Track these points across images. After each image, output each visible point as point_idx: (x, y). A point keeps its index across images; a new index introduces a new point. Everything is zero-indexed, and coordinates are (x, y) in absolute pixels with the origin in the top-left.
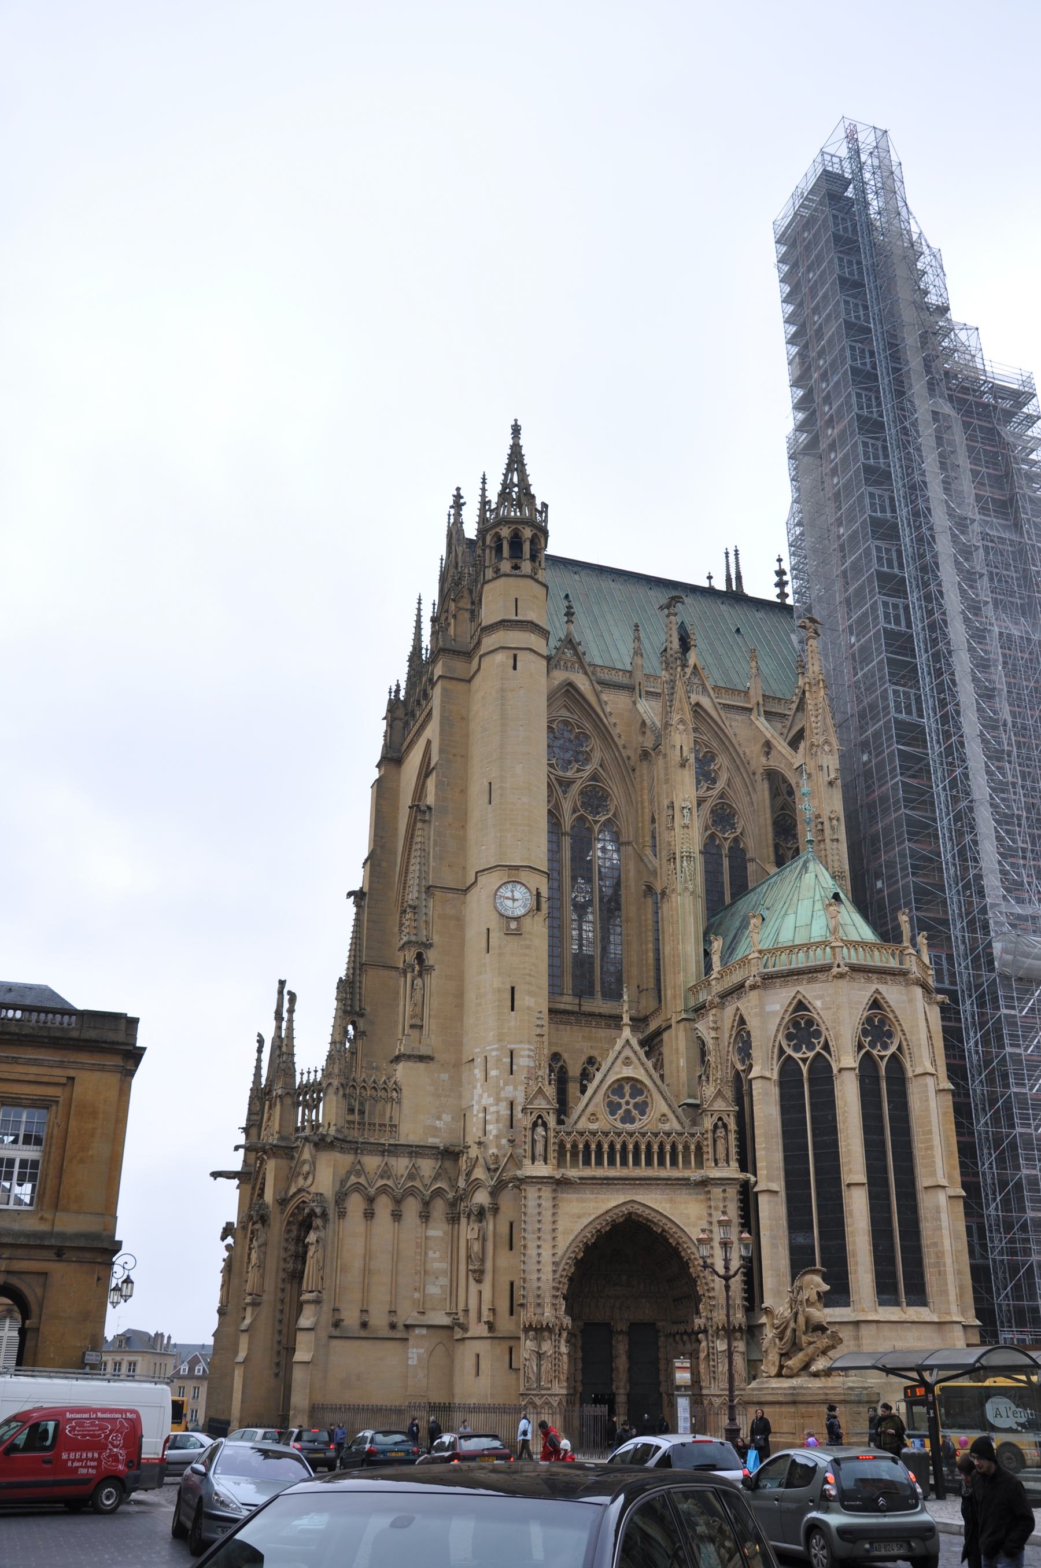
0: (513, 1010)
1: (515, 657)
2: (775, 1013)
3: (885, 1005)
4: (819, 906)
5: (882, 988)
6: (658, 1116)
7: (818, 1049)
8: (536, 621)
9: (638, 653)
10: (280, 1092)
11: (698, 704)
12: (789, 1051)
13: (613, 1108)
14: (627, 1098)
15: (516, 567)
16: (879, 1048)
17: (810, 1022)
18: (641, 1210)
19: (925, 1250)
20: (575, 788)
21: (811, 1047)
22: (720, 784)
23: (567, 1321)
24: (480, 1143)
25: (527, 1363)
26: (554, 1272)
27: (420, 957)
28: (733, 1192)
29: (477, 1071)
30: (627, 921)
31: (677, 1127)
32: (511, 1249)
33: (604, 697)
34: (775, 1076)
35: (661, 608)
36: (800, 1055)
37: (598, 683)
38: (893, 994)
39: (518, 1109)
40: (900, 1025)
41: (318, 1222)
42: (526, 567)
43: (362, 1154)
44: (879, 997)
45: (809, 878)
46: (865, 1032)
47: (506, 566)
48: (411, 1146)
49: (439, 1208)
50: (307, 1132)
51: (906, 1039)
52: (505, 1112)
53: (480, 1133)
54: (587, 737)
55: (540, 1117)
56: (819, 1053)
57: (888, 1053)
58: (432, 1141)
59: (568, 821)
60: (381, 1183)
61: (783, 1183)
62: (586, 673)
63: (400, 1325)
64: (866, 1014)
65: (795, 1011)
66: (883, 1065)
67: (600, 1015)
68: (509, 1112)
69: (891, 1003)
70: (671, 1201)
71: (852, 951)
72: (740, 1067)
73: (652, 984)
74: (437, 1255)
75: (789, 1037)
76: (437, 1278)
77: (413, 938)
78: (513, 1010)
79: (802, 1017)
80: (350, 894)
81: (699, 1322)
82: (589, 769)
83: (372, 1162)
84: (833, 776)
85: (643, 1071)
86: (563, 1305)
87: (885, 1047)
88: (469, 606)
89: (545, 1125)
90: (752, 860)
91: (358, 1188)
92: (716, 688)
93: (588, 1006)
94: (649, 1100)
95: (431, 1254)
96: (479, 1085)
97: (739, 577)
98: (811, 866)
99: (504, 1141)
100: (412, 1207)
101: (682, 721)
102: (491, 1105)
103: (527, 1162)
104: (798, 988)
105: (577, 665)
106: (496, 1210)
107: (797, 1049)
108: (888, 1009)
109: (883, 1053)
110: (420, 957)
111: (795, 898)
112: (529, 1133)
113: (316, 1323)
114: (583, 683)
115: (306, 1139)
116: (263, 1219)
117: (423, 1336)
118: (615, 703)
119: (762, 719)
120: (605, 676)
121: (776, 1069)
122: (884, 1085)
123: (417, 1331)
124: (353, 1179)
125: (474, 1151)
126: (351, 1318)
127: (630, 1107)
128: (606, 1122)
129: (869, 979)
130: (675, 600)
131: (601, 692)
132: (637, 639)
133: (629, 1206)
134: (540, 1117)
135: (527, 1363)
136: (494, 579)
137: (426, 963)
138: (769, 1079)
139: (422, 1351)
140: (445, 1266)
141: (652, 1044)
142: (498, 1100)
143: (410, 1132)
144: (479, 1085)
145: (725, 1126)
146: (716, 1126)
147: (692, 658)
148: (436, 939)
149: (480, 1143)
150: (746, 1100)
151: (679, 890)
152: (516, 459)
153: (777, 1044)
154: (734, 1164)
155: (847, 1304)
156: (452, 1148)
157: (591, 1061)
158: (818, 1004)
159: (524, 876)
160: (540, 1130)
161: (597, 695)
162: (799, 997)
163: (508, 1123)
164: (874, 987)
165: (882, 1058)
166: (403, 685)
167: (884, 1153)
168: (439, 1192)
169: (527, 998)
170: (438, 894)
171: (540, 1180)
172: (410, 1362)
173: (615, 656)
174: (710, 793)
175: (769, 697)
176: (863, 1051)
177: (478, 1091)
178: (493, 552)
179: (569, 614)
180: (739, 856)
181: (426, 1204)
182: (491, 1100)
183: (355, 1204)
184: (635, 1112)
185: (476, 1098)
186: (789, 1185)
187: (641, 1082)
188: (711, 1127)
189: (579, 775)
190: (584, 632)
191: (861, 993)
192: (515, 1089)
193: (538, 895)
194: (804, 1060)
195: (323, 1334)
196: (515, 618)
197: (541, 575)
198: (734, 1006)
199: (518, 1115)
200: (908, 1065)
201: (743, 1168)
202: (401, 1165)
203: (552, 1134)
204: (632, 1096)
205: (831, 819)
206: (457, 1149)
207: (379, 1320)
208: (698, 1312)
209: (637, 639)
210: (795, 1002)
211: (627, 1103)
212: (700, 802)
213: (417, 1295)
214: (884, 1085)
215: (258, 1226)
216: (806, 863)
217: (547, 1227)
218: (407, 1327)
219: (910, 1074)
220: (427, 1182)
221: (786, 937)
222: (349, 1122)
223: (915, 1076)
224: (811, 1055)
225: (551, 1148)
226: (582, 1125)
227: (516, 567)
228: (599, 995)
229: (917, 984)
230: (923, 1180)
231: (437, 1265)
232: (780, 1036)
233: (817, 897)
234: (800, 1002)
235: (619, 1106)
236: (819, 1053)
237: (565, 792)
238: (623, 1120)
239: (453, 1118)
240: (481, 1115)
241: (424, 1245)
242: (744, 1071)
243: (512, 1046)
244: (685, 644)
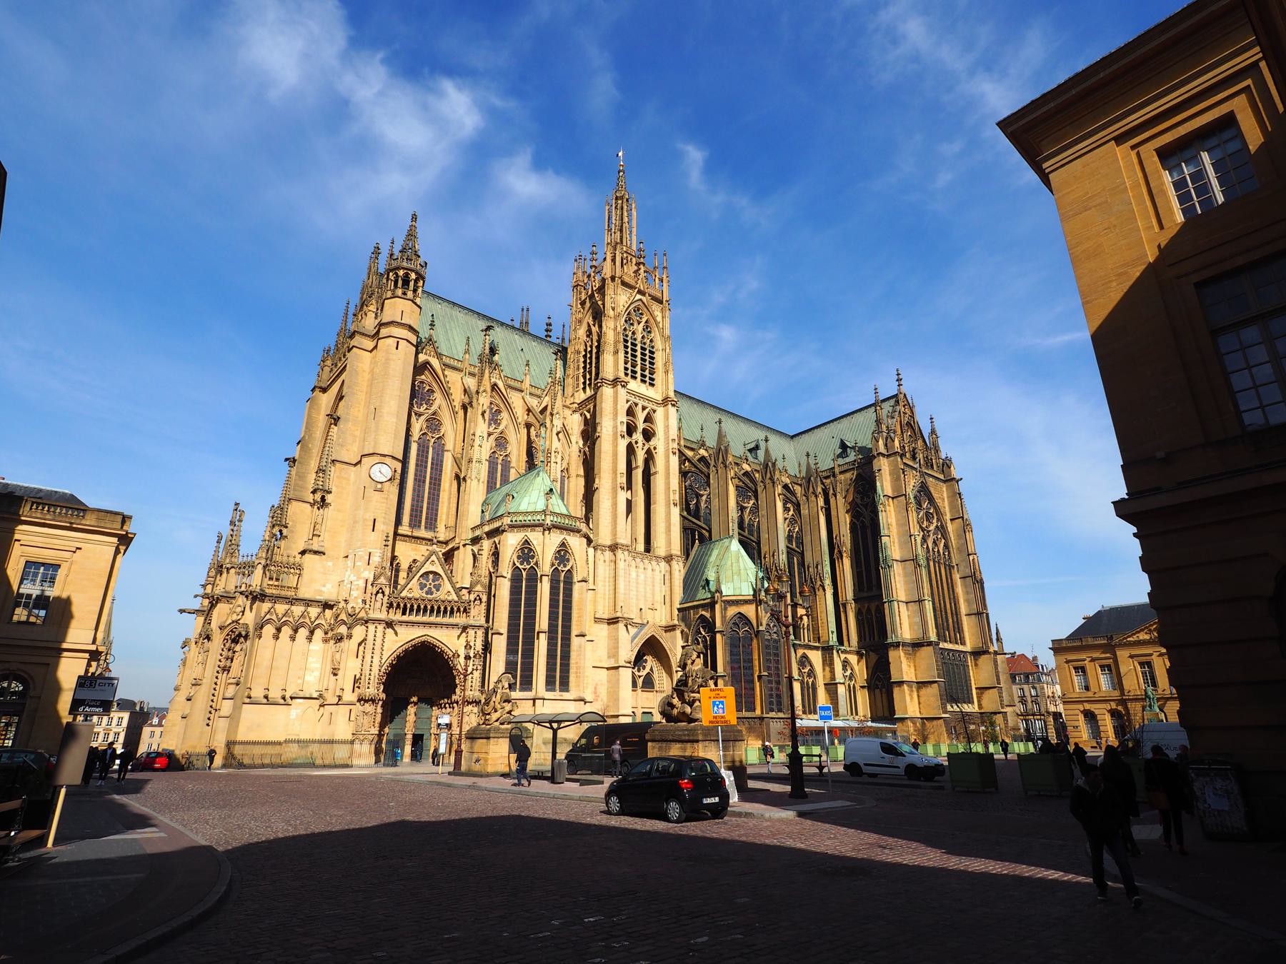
0: (373, 531)
1: (398, 342)
2: (512, 545)
4: (542, 494)
5: (567, 538)
6: (446, 592)
7: (532, 564)
8: (412, 325)
9: (467, 352)
10: (229, 566)
11: (495, 384)
12: (518, 564)
13: (422, 587)
14: (430, 581)
15: (404, 294)
17: (531, 550)
18: (430, 639)
19: (571, 665)
20: (423, 418)
21: (529, 563)
22: (501, 427)
23: (383, 696)
24: (346, 601)
25: (358, 718)
26: (380, 671)
27: (323, 498)
28: (480, 633)
29: (349, 562)
30: (443, 491)
31: (456, 599)
32: (357, 657)
33: (446, 373)
34: (509, 576)
35: (482, 331)
36: (523, 567)
37: (444, 365)
38: (576, 543)
39: (369, 583)
41: (242, 640)
42: (410, 294)
43: (275, 602)
45: (539, 480)
46: (556, 558)
47: (399, 292)
48: (305, 600)
49: (319, 634)
50: (243, 589)
52: (362, 584)
53: (347, 596)
54: (433, 391)
55: (381, 588)
56: (532, 567)
57: (566, 569)
58: (318, 598)
59: (416, 434)
60: (284, 619)
61: (506, 630)
62: (437, 358)
63: (287, 697)
64: (558, 549)
65: (522, 545)
66: (563, 574)
67: (423, 539)
68: (365, 585)
69: (571, 545)
70: (447, 636)
71: (555, 518)
72: (492, 570)
73: (453, 524)
74: (314, 660)
75: (519, 557)
76: (313, 672)
77: (321, 487)
78: (373, 531)
79: (526, 548)
80: (286, 460)
81: (454, 697)
82: (433, 408)
83: (281, 608)
84: (559, 430)
85: (441, 569)
86: (382, 687)
87: (565, 566)
88: (375, 310)
89: (383, 593)
90: (513, 467)
91: (269, 621)
92: (505, 376)
93: (416, 534)
94: (442, 584)
95: (310, 659)
96: (349, 569)
97: (527, 323)
98: (541, 473)
99: (360, 601)
100: (303, 632)
101: (484, 391)
102: (354, 581)
103: (371, 612)
104: (527, 534)
105: (432, 353)
106: (350, 637)
109: (563, 569)
110: (323, 498)
111: (531, 489)
112: (374, 597)
113: (234, 695)
114: (435, 363)
115: (241, 593)
116: (208, 638)
117: (300, 703)
118: (452, 377)
119: (528, 396)
120: (447, 361)
121: (510, 572)
122: (562, 585)
123: (298, 700)
124: (268, 617)
125: (342, 604)
126: (257, 693)
127: (432, 586)
128: (417, 593)
129: (561, 533)
130: (489, 328)
131: (444, 370)
132: (468, 344)
133: (424, 638)
134: (381, 588)
135: (358, 718)
136: (391, 298)
137: (326, 502)
139: (299, 711)
140: (318, 666)
141: (449, 557)
142: (359, 578)
143: (305, 593)
144: (349, 569)
145: (480, 599)
146: (475, 599)
147: (496, 358)
148: (334, 489)
149: (346, 601)
150: (493, 587)
151: (473, 478)
152: (411, 235)
153: (512, 560)
154: (483, 620)
155: (530, 690)
156: (330, 603)
157: (415, 561)
158: (535, 542)
159: (388, 460)
160: (380, 595)
161: (443, 371)
163: (364, 591)
164: (563, 537)
165: (563, 571)
166: (333, 348)
167: (558, 617)
168: (318, 626)
169: (382, 526)
170: (338, 465)
171: (379, 621)
172: (291, 717)
173: (455, 352)
174: (495, 431)
175: (532, 386)
176: (554, 567)
177: (348, 573)
178: (393, 283)
179: (432, 325)
180: (506, 465)
181: (312, 632)
182: (355, 578)
183: (269, 630)
184: (434, 590)
185: (347, 576)
186: (509, 631)
187: (439, 575)
188: (473, 599)
189: (427, 411)
190: (439, 335)
191: (555, 538)
192: (370, 573)
193: (395, 471)
194: (524, 569)
195: (239, 702)
196: (399, 321)
197: (418, 301)
198: (493, 540)
199: (369, 587)
200: (575, 575)
201: (487, 621)
202: (298, 610)
203: (386, 598)
204: (433, 581)
205: (555, 452)
206: (332, 603)
207: (275, 694)
208: (455, 693)
209: (468, 344)
210: (524, 540)
211: (430, 584)
212: (489, 435)
213: (300, 681)
214: (562, 585)
215: (206, 640)
216: (539, 471)
217: (378, 647)
218: (292, 698)
219: (575, 580)
220: (313, 620)
221: (523, 508)
222: (268, 585)
223: (578, 582)
224: (528, 567)
225: (385, 605)
226: (403, 594)
227: (404, 294)
228: (423, 527)
229: (584, 537)
230: (574, 632)
231: (314, 665)
232: (515, 558)
233: (542, 489)
234: (526, 540)
235: (425, 585)
236: (532, 567)
237: (417, 420)
238: (427, 593)
239: (332, 587)
240: (350, 586)
241: (306, 655)
242: (493, 573)
243: (370, 551)
244: (493, 351)
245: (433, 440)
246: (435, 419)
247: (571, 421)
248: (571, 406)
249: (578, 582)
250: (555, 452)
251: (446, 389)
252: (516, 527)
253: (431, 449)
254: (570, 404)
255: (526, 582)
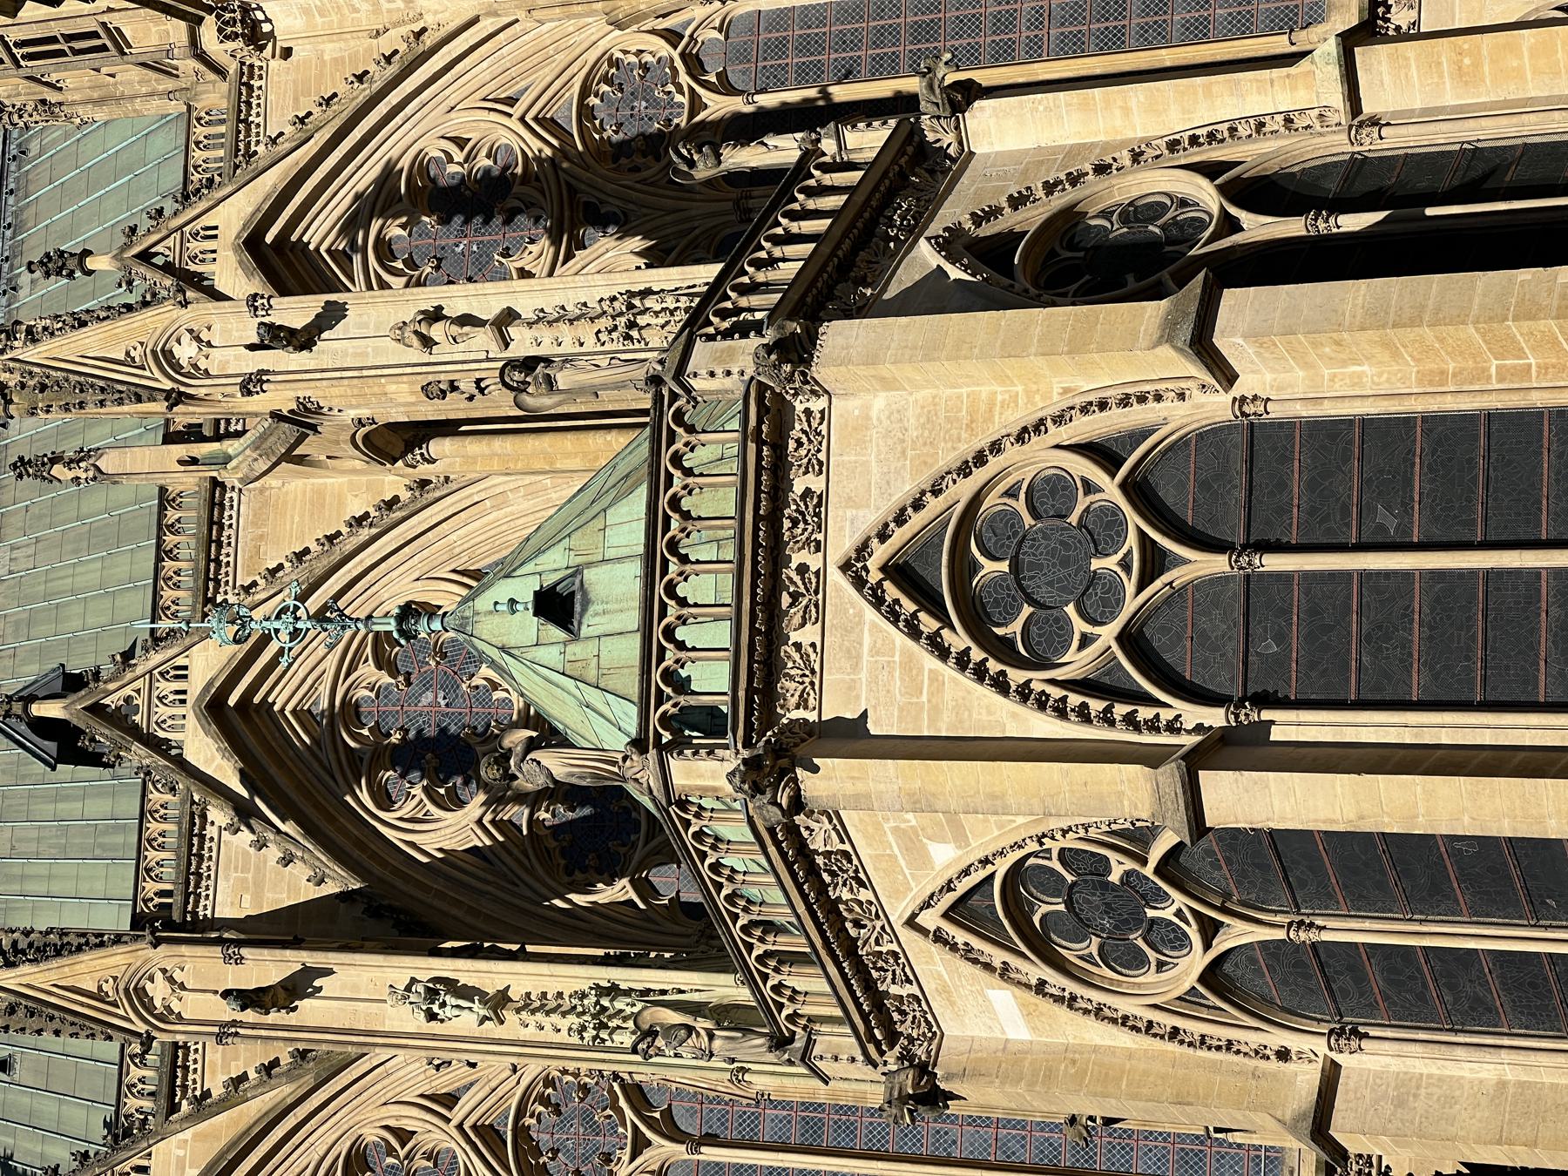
3: (916, 520)
5: (841, 543)
16: (1111, 563)
34: (1312, 1045)
40: (996, 447)
44: (880, 553)
51: (1059, 420)
64: (958, 640)
69: (904, 490)
79: (1018, 910)
107: (1170, 939)
108: (934, 505)
138: (1331, 1075)
161: (204, 1106)
162: (930, 919)
164: (837, 580)
219: (1214, 406)
245: (663, 1150)
246: (520, 1132)
247: (330, 50)
248: (232, 67)
249: (1227, 376)
250: (427, 342)
251: (309, 1081)
252: (878, 999)
253: (710, 1154)
254: (220, 71)
255: (1325, 901)
